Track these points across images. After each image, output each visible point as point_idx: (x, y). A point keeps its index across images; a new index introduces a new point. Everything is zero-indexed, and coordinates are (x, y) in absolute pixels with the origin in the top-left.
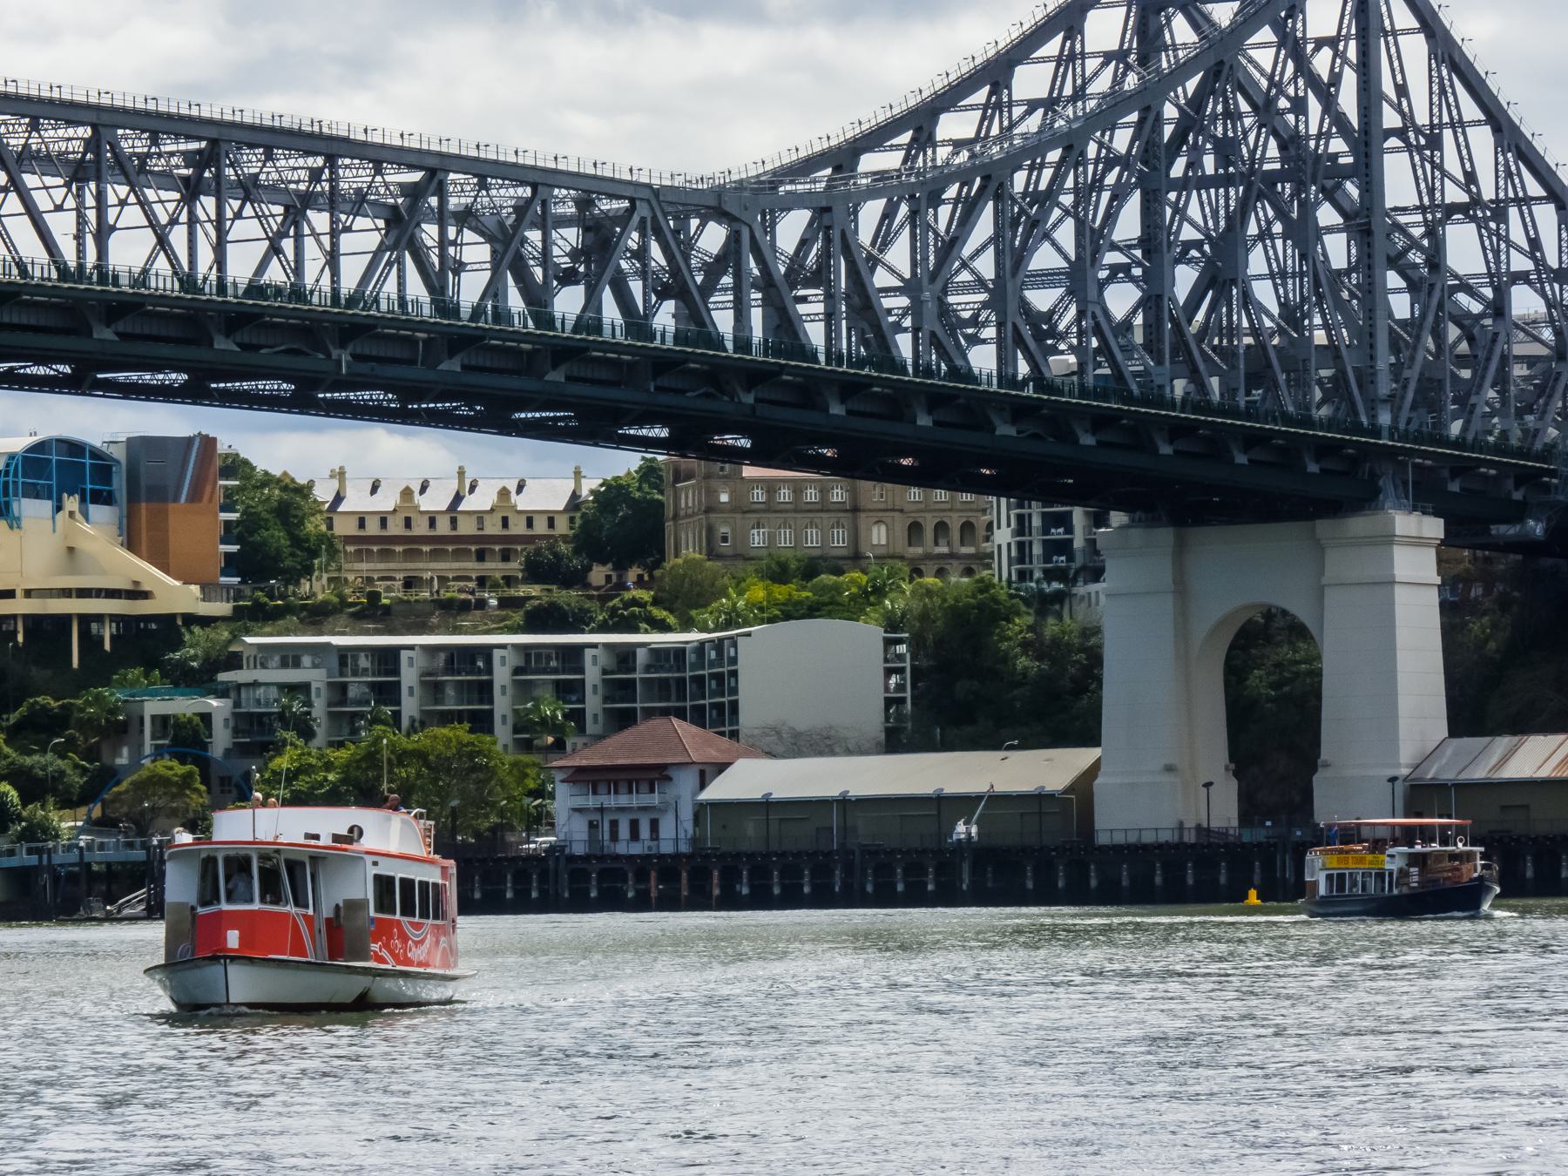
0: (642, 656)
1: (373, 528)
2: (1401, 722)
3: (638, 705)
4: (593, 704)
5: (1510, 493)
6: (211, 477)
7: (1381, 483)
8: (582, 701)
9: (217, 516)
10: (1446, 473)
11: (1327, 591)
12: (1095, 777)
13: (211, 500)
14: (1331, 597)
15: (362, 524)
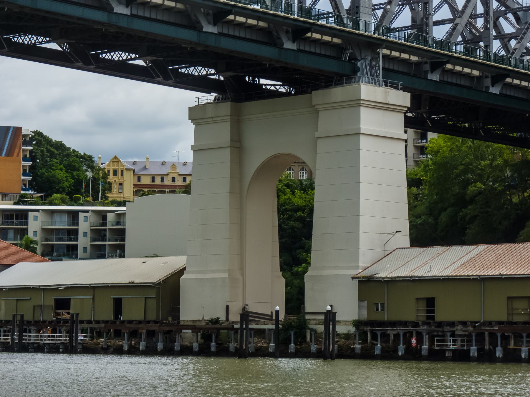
0: (110, 217)
1: (158, 181)
2: (361, 235)
3: (107, 243)
4: (83, 242)
5: (488, 88)
6: (18, 146)
7: (359, 64)
8: (77, 240)
9: (21, 163)
10: (427, 67)
11: (320, 143)
12: (183, 274)
13: (18, 156)
14: (321, 144)
15: (153, 180)
